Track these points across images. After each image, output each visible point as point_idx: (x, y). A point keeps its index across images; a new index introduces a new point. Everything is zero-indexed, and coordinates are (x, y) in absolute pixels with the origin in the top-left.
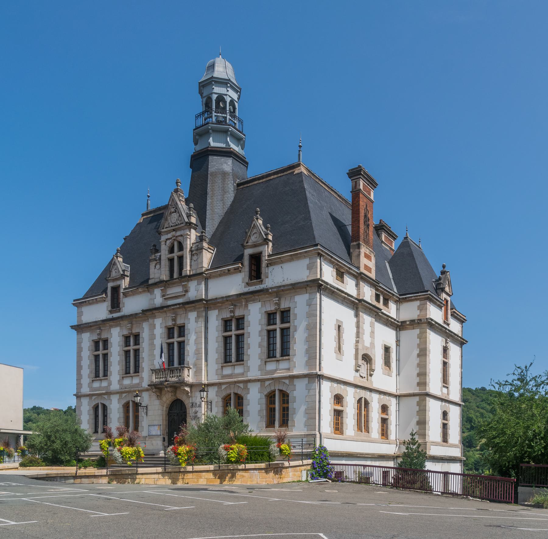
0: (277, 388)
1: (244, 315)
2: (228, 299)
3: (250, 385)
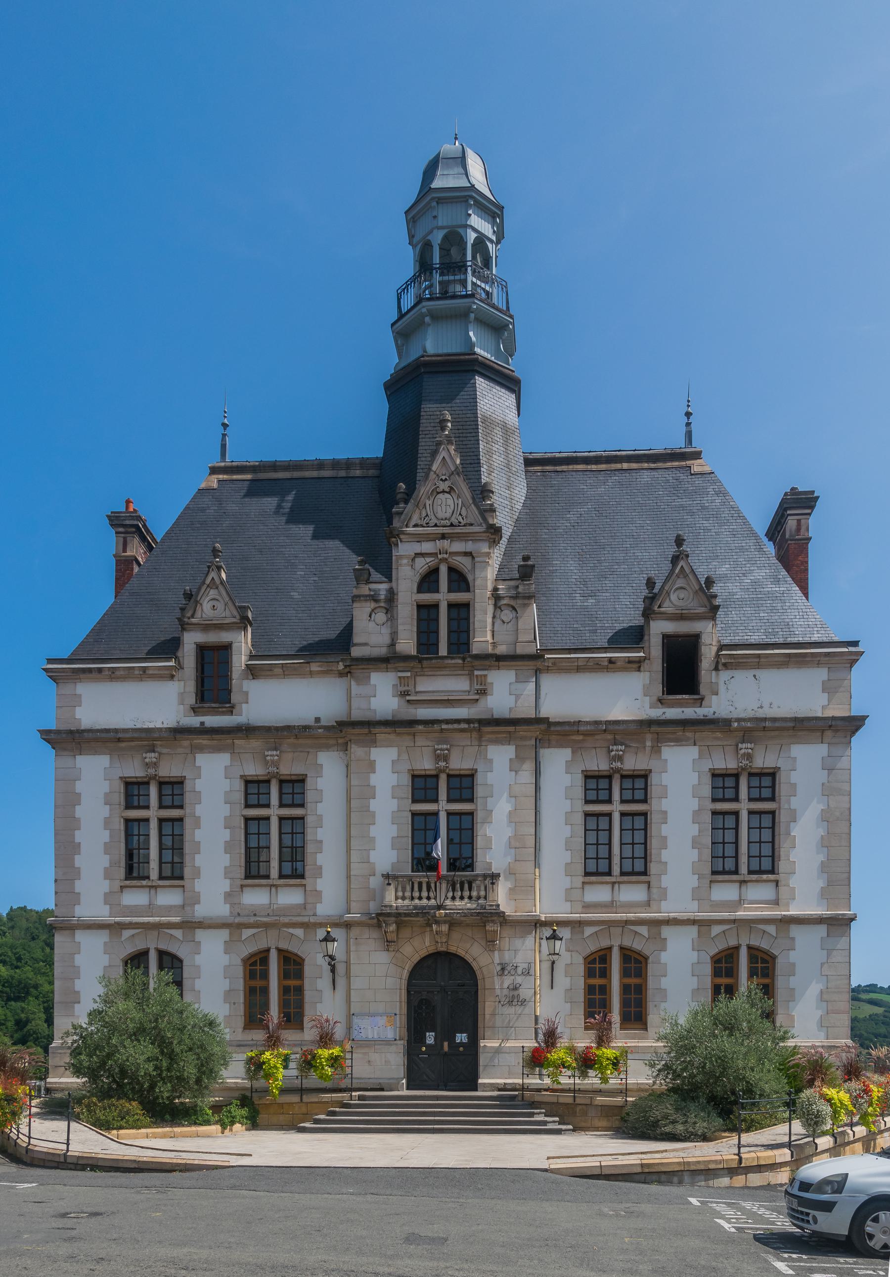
0: (744, 942)
1: (650, 771)
2: (611, 727)
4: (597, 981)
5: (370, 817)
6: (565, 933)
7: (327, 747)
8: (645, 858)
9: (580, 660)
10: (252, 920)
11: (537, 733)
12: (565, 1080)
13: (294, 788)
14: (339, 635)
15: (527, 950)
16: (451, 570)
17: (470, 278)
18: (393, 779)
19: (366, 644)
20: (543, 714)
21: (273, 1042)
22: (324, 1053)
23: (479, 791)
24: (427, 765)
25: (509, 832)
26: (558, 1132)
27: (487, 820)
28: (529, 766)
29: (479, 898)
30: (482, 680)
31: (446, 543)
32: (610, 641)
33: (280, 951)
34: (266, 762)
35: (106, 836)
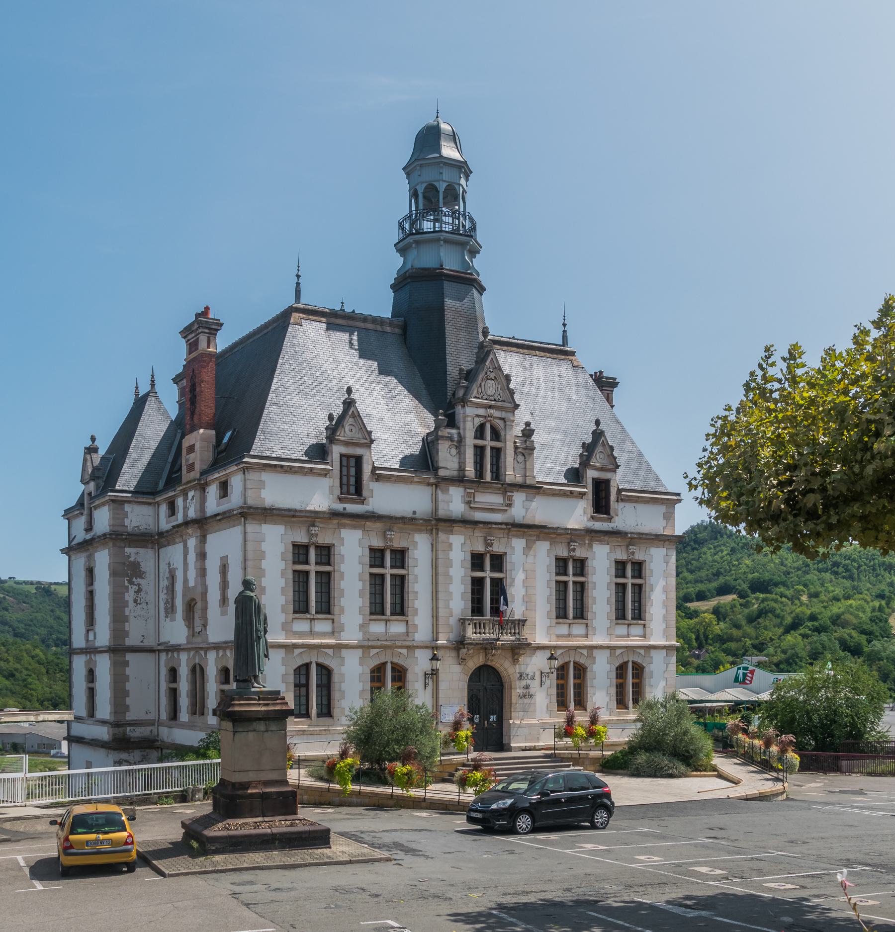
3: (596, 653)
16: (492, 427)
19: (446, 468)
27: (512, 585)
30: (510, 498)
35: (282, 582)
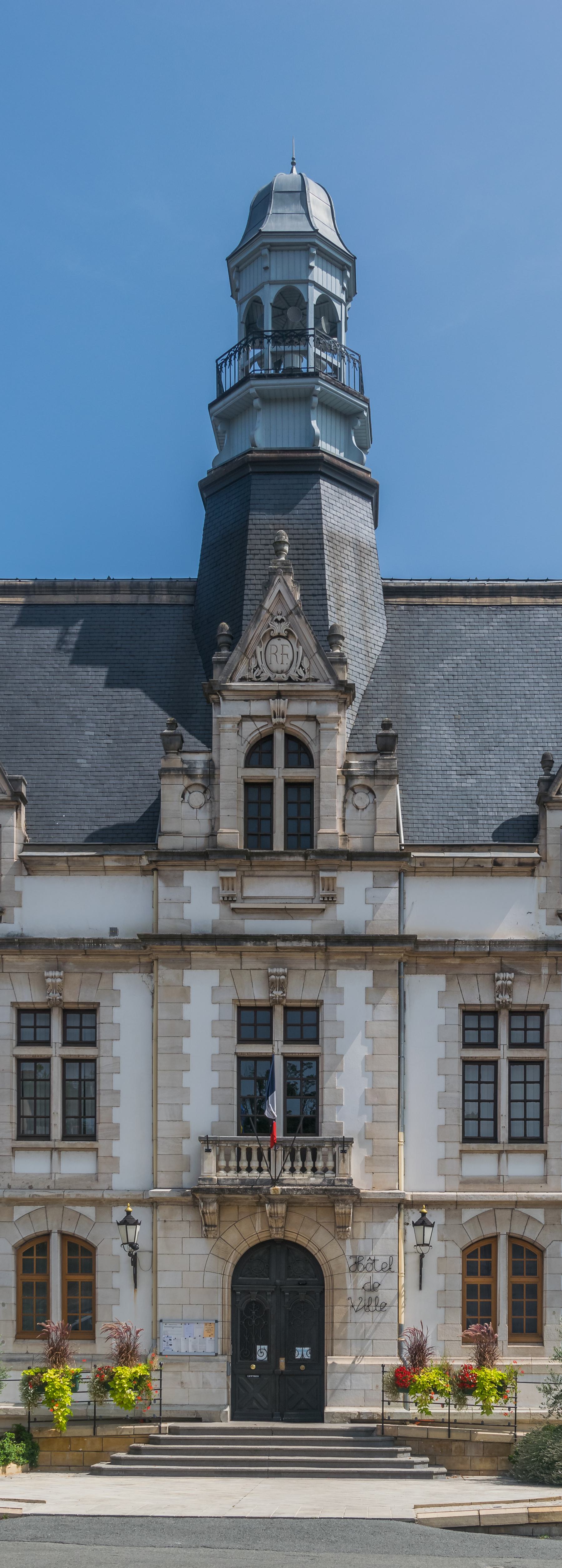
1: (547, 1006)
2: (496, 949)
4: (478, 1280)
5: (182, 1062)
6: (437, 1216)
7: (126, 968)
8: (541, 1119)
9: (455, 859)
10: (27, 1194)
11: (400, 954)
12: (436, 1409)
13: (83, 1021)
14: (142, 819)
15: (387, 1239)
16: (289, 737)
17: (312, 350)
18: (213, 1012)
19: (177, 833)
20: (409, 930)
21: (57, 1356)
22: (125, 1372)
23: (326, 1030)
24: (257, 993)
25: (364, 1084)
26: (428, 1476)
27: (336, 1068)
28: (391, 996)
29: (325, 1170)
30: (330, 884)
31: (282, 704)
32: (496, 835)
33: (63, 1235)
34: (46, 986)
